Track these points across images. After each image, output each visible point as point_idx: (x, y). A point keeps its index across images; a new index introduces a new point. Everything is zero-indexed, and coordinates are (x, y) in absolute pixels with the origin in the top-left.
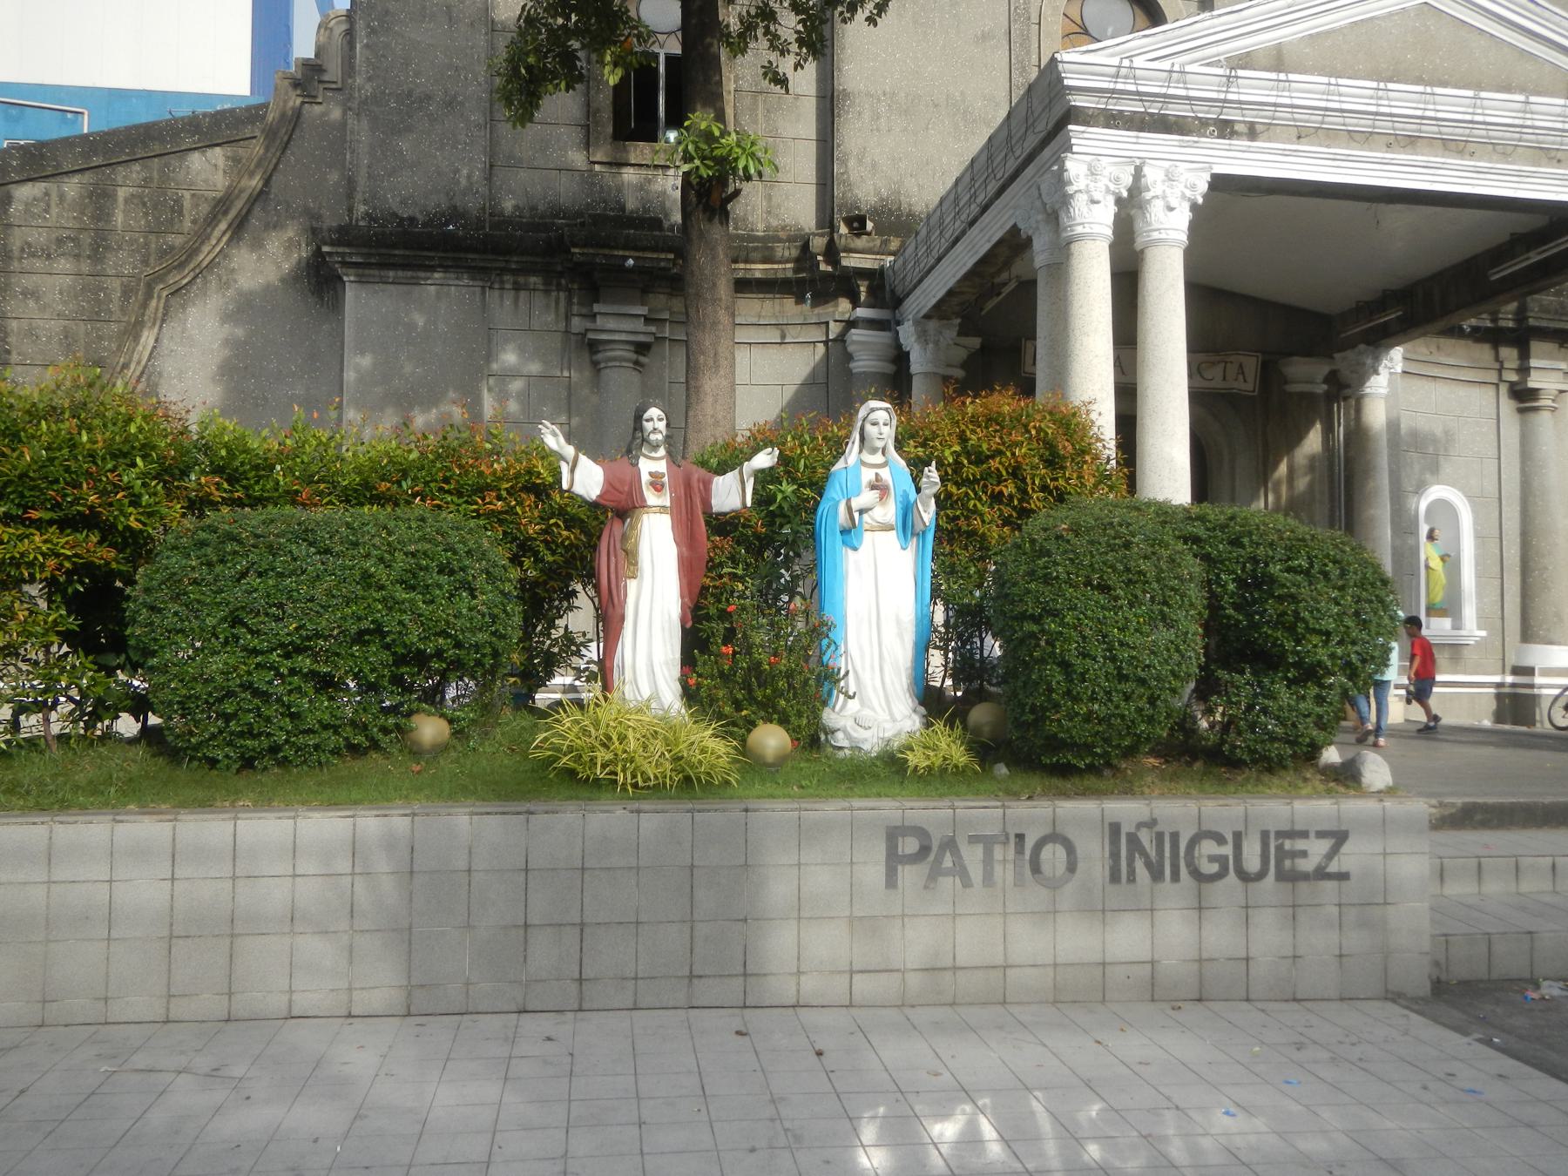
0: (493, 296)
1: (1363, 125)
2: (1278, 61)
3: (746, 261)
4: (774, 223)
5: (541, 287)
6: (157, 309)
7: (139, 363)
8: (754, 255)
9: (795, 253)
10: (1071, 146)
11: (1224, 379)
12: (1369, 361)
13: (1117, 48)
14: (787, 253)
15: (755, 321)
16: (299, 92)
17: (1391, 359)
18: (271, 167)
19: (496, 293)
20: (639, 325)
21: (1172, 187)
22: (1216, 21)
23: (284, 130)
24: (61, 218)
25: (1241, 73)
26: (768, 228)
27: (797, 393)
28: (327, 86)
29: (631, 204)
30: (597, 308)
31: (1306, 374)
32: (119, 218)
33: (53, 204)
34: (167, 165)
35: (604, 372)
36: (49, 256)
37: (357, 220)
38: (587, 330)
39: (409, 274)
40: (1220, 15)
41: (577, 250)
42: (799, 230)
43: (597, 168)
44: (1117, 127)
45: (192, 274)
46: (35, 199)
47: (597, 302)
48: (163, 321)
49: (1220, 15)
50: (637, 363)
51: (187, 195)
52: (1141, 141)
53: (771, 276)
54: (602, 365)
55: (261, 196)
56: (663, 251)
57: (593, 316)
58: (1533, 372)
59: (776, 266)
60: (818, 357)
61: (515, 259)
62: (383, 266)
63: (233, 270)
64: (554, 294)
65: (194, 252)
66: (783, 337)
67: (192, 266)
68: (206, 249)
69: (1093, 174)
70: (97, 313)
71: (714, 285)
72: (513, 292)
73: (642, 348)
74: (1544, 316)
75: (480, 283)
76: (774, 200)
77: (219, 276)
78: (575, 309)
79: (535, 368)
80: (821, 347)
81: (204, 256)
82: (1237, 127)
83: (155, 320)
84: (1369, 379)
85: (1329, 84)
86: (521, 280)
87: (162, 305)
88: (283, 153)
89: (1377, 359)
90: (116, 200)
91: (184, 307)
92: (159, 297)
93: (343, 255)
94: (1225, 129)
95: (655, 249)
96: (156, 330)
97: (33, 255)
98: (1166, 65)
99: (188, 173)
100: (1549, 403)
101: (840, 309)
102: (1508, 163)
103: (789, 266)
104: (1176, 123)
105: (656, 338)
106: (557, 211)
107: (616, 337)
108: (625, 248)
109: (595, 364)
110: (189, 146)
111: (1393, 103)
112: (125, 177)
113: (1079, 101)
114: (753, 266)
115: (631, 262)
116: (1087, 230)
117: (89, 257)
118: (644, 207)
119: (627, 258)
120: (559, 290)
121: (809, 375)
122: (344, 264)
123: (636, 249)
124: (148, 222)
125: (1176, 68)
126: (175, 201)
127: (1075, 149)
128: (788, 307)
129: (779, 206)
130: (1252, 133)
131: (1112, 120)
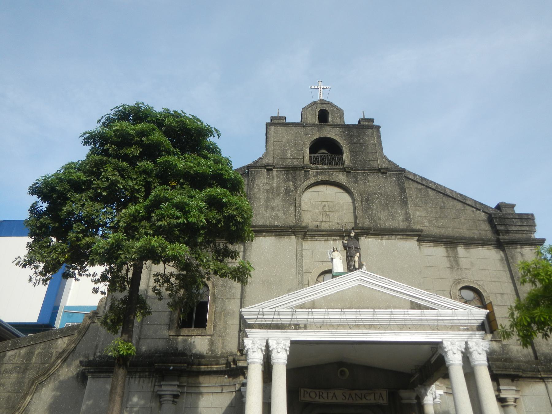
0: (132, 381)
1: (337, 322)
2: (313, 305)
3: (211, 365)
4: (224, 351)
5: (147, 377)
6: (34, 388)
7: (24, 407)
8: (214, 363)
9: (225, 362)
10: (247, 335)
11: (375, 399)
12: (423, 391)
13: (260, 306)
14: (223, 362)
15: (214, 385)
16: (90, 320)
17: (431, 390)
18: (78, 342)
19: (133, 380)
20: (176, 388)
21: (279, 345)
22: (290, 296)
23: (83, 332)
24: (18, 361)
25: (297, 310)
26: (222, 353)
27: (226, 410)
28: (99, 318)
29: (180, 347)
30: (162, 383)
31: (407, 395)
32: (34, 360)
33: (16, 356)
34: (51, 343)
35: (164, 405)
36: (11, 372)
37: (96, 358)
38: (158, 391)
39: (107, 374)
40: (291, 294)
41: (156, 365)
42: (232, 353)
43: (171, 337)
44: (262, 329)
45: (47, 377)
46: (12, 355)
47: (163, 381)
48: (35, 392)
49: (291, 294)
50: (173, 401)
51: (55, 352)
52: (269, 332)
53: (219, 369)
54: (162, 403)
55: (73, 351)
56: (183, 363)
57: (161, 386)
58: (502, 391)
59: (220, 366)
60: (233, 397)
61: (140, 368)
62: (100, 372)
63: (59, 375)
64: (151, 379)
65: (49, 370)
66: (222, 390)
67: (47, 374)
68: (53, 369)
69: (253, 343)
70: (19, 390)
71: (116, 388)
72: (138, 379)
73: (176, 396)
74: (498, 369)
75: (128, 376)
76: (224, 344)
77: (55, 377)
78: (156, 384)
79: (142, 402)
80: (234, 393)
81: (51, 372)
82: (300, 326)
83: (32, 392)
84: (424, 397)
85: (325, 311)
86: (142, 374)
87: (35, 387)
88: (82, 338)
89: (426, 391)
90: (34, 354)
91: (42, 388)
92: (35, 386)
93: (88, 369)
94: (297, 327)
95: (180, 363)
96: (32, 396)
97: (7, 372)
98: (274, 310)
99: (57, 345)
100: (512, 403)
101: (240, 380)
102: (392, 330)
103: (225, 366)
104: (281, 326)
105: (181, 393)
106: (157, 351)
107: (167, 393)
108: (171, 363)
109: (160, 402)
110: (58, 337)
111: (346, 315)
112: (39, 347)
113: (249, 322)
114: (213, 367)
115: (172, 367)
116: (252, 361)
117: (22, 372)
118: (184, 348)
119: (171, 366)
120: (153, 377)
121: (230, 403)
122: (89, 372)
123: (174, 363)
124: (41, 361)
125: (277, 310)
126: (51, 354)
127: (248, 336)
128: (226, 380)
129: (226, 346)
130: (305, 327)
131: (261, 327)
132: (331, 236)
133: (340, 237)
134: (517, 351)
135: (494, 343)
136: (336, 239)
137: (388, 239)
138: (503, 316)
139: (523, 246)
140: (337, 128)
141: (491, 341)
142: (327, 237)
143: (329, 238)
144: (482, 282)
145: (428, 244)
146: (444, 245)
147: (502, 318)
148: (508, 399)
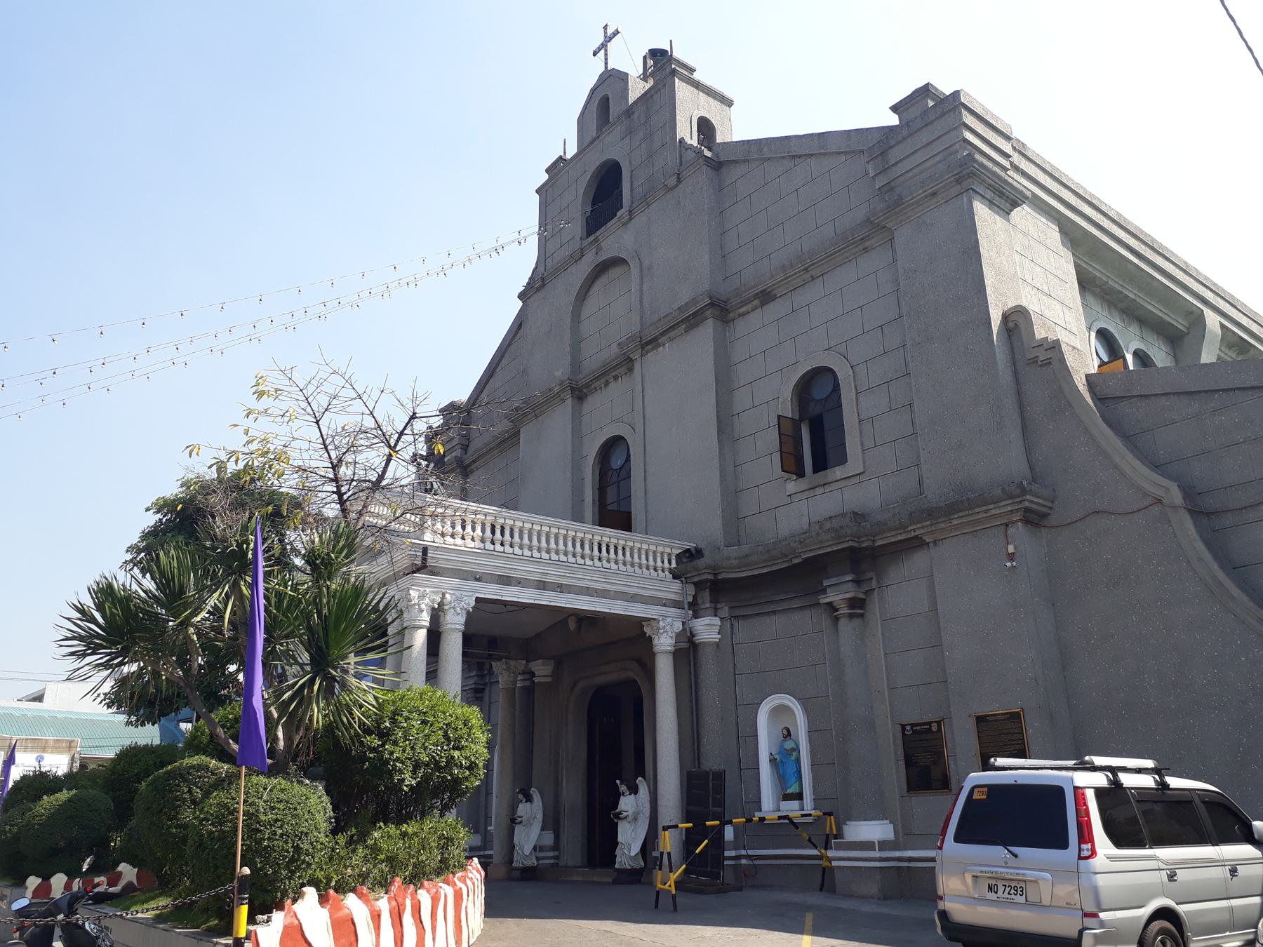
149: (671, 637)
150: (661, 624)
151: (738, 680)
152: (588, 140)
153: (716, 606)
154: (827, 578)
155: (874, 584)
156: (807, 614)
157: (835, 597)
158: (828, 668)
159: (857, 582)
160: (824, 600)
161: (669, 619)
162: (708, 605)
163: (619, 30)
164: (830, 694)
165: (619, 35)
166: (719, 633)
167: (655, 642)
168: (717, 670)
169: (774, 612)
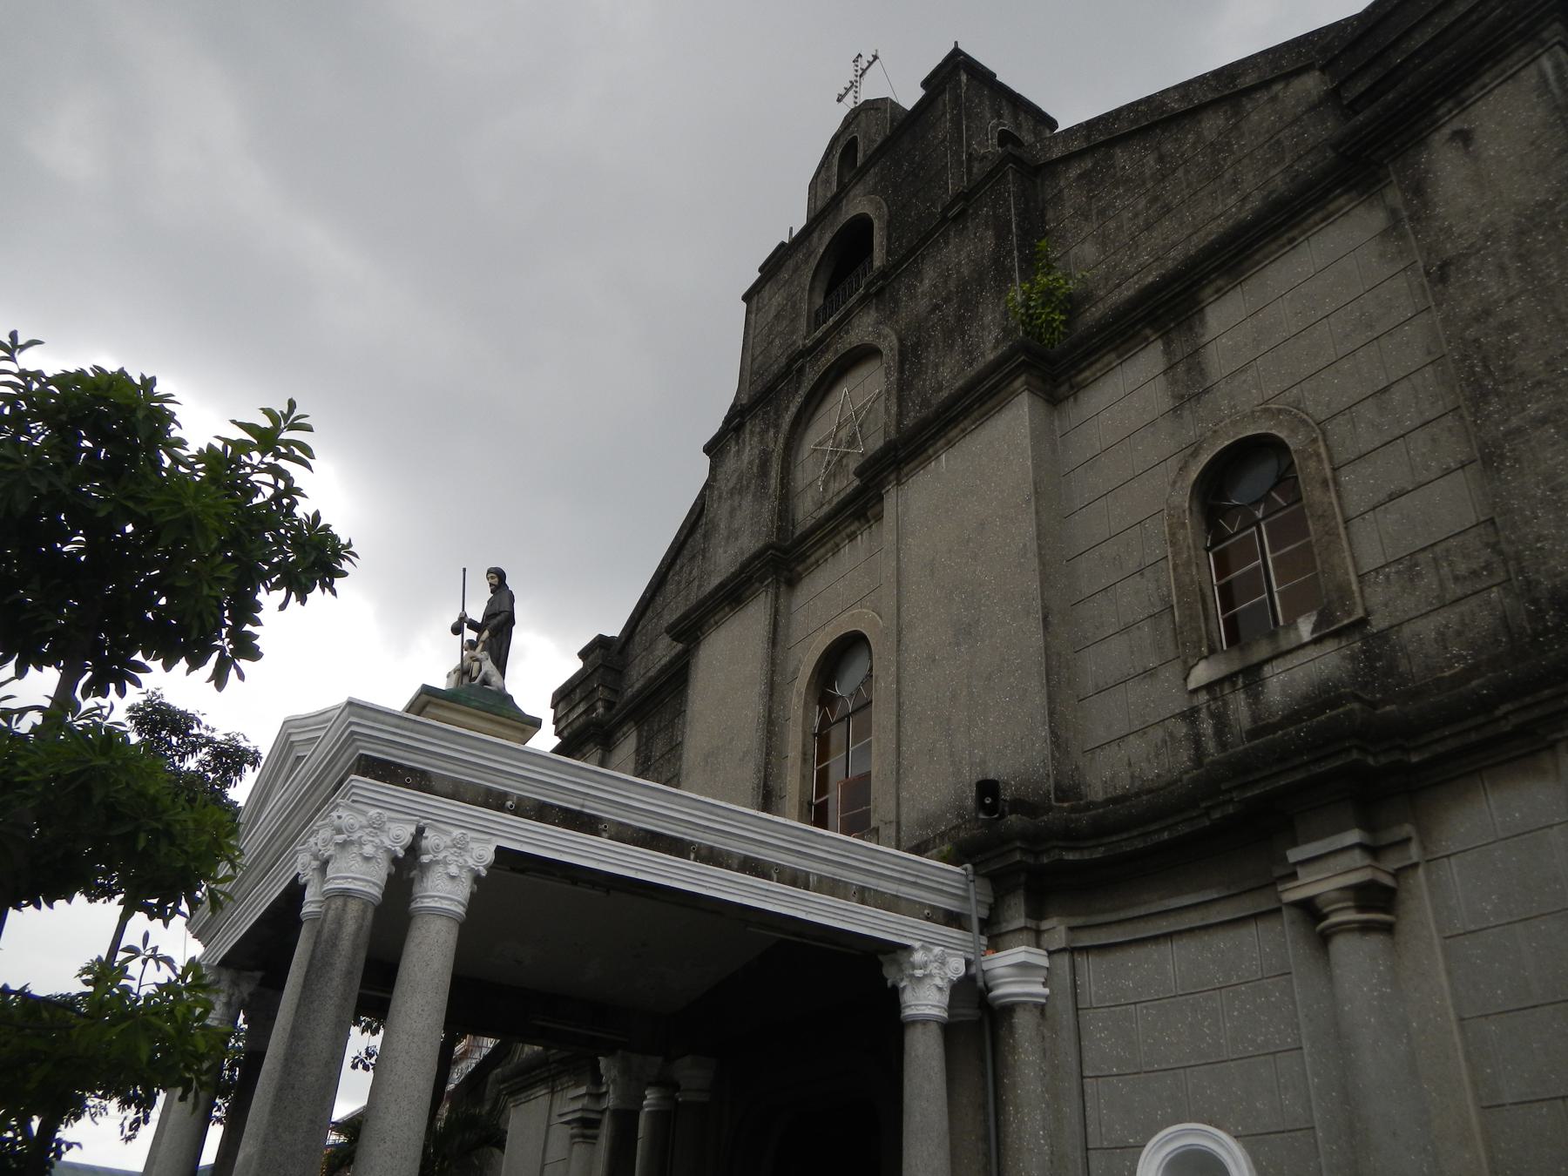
58: (1300, 871)
100: (1352, 916)
132: (834, 531)
133: (858, 519)
134: (1442, 638)
135: (1330, 646)
136: (855, 532)
137: (950, 444)
138: (1382, 496)
139: (1464, 94)
140: (868, 171)
141: (1316, 642)
142: (832, 542)
143: (837, 539)
144: (1295, 391)
145: (1098, 365)
146: (1155, 332)
147: (1374, 508)
148: (1319, 902)
149: (940, 989)
150: (918, 957)
151: (1088, 1090)
152: (820, 204)
153: (1038, 926)
154: (1295, 844)
155: (1414, 852)
156: (1249, 933)
157: (1311, 884)
158: (1308, 1059)
159: (1373, 851)
160: (1294, 893)
161: (937, 950)
162: (1020, 922)
163: (879, 55)
164: (1317, 1126)
165: (877, 61)
166: (1045, 984)
167: (908, 997)
168: (1041, 1069)
169: (1169, 936)
